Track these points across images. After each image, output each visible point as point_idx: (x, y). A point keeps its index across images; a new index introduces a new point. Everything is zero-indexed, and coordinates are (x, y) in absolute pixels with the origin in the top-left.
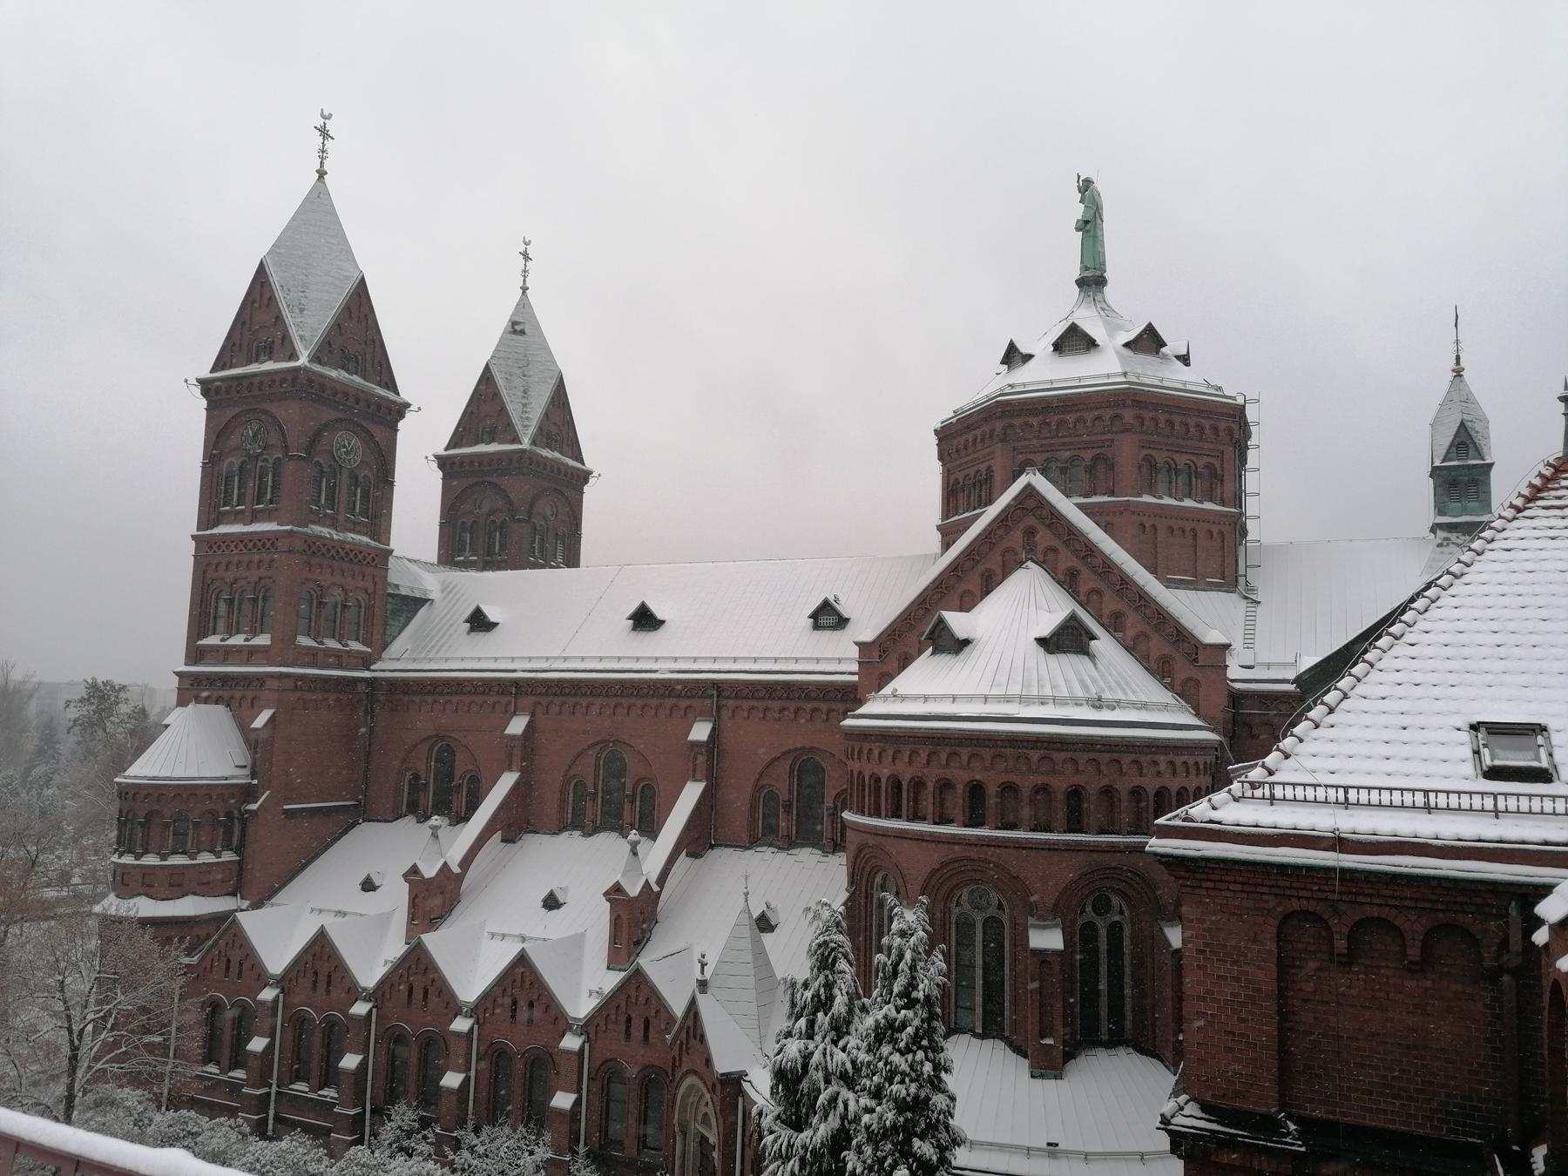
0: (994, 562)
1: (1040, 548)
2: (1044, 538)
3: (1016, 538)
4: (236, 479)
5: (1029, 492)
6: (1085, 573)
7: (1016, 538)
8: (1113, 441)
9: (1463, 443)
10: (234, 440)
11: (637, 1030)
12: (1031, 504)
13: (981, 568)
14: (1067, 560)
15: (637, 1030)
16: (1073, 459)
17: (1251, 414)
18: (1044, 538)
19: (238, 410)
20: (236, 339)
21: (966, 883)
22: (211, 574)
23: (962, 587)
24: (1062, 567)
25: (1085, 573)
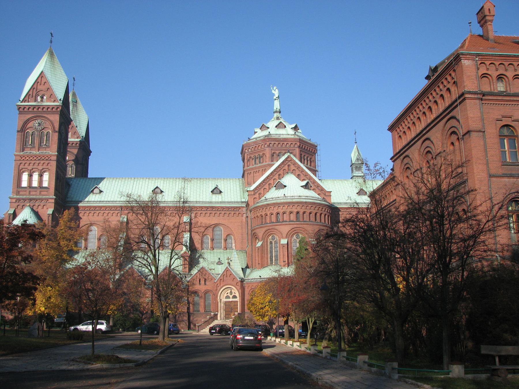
0: (281, 172)
1: (292, 170)
2: (292, 167)
3: (286, 167)
4: (45, 137)
5: (288, 157)
6: (302, 175)
7: (286, 167)
8: (295, 149)
9: (358, 159)
10: (30, 125)
11: (202, 282)
12: (289, 159)
13: (278, 174)
14: (298, 172)
15: (202, 282)
16: (280, 153)
17: (318, 148)
18: (292, 167)
19: (33, 115)
20: (31, 93)
21: (294, 234)
22: (21, 167)
23: (274, 178)
24: (297, 174)
25: (302, 175)
